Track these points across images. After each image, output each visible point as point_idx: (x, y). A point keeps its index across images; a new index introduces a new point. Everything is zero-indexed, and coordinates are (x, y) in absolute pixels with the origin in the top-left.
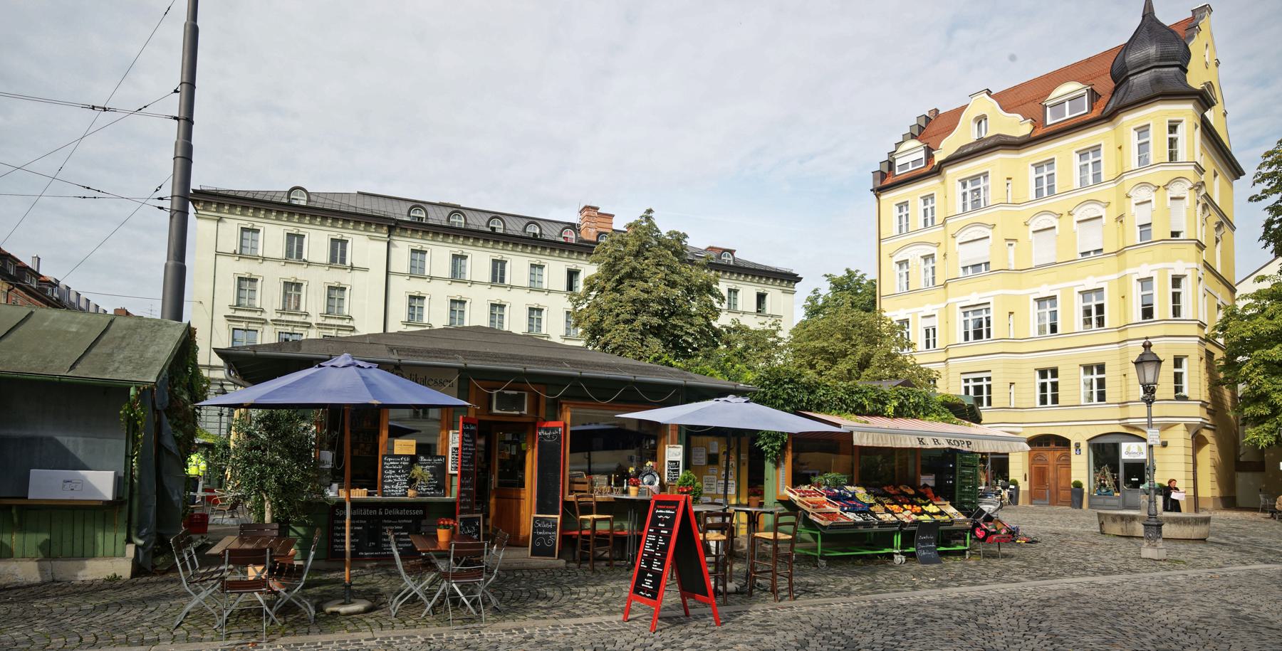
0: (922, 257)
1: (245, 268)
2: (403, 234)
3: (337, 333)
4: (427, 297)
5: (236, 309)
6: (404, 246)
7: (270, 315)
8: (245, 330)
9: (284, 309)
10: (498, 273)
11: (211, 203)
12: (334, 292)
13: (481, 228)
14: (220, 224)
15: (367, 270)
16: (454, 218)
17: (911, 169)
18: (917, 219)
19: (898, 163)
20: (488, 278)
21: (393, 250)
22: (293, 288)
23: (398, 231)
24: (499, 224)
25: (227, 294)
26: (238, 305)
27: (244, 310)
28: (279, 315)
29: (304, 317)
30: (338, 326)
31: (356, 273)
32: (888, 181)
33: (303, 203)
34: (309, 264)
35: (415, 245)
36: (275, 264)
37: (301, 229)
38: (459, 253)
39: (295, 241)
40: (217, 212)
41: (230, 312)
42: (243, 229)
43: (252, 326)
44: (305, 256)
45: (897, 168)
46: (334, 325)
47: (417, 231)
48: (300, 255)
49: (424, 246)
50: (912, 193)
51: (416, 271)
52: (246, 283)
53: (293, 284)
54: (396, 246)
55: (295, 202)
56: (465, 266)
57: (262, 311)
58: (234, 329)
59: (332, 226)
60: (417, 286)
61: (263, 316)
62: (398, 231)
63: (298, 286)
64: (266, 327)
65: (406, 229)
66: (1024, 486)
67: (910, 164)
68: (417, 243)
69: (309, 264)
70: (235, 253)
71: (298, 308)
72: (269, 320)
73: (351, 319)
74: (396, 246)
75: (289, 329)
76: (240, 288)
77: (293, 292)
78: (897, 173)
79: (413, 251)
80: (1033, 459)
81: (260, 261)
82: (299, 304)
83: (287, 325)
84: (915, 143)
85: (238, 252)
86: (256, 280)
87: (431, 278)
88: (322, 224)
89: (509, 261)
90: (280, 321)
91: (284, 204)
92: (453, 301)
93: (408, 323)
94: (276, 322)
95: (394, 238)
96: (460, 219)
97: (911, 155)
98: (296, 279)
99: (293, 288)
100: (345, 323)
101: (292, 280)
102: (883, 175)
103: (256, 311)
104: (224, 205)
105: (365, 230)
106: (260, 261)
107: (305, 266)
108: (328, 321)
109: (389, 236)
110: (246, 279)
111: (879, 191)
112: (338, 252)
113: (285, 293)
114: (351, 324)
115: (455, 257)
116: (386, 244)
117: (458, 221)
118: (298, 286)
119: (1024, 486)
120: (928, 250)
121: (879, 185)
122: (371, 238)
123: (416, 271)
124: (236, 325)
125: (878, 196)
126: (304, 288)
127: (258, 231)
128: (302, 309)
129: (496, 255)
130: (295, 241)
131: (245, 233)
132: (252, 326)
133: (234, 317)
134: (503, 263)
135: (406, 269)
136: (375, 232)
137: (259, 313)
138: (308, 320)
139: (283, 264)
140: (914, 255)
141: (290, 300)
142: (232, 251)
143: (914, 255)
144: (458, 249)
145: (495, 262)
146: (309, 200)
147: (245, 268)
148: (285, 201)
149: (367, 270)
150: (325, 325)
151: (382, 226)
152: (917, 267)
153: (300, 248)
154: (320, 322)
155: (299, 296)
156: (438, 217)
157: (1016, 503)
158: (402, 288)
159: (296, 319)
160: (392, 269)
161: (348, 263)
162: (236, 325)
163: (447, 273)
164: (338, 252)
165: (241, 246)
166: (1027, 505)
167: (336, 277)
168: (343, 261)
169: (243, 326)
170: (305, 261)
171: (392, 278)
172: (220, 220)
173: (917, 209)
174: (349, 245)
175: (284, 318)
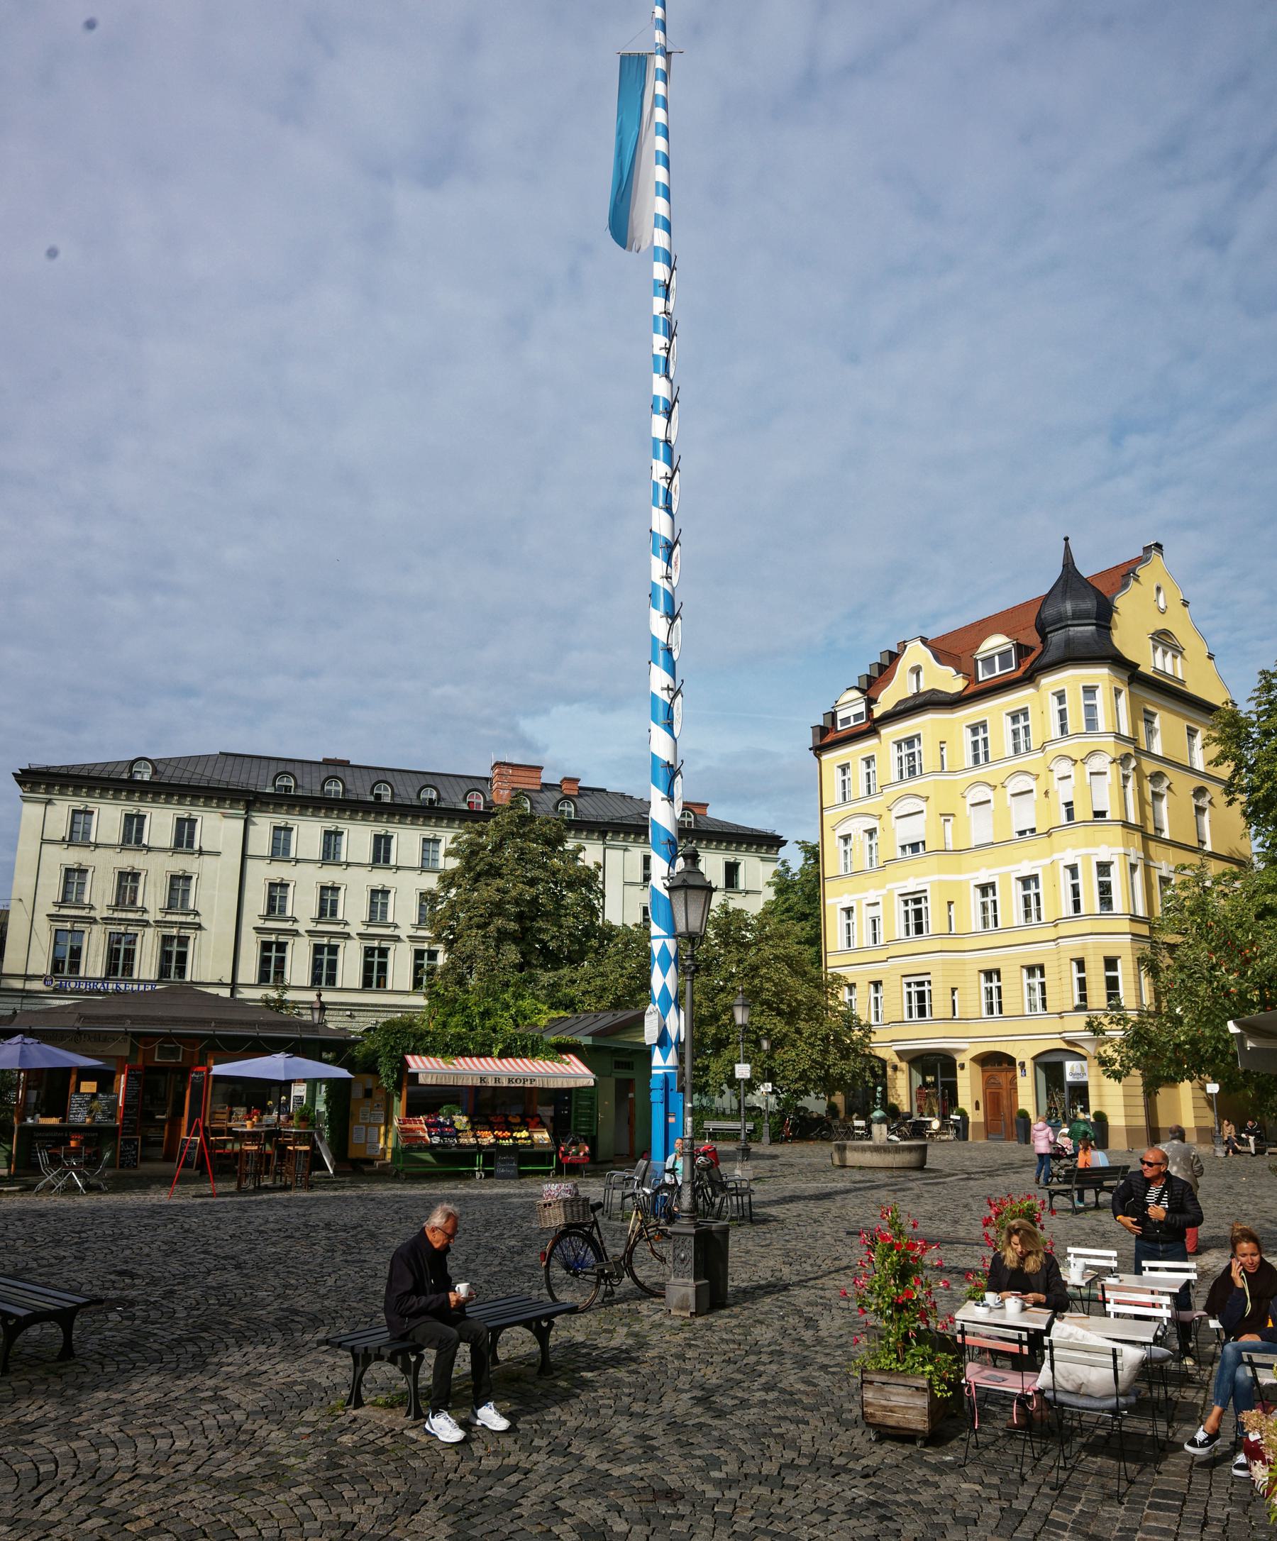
0: (866, 831)
1: (74, 857)
2: (264, 809)
3: (178, 932)
4: (292, 885)
5: (60, 907)
6: (264, 825)
7: (101, 912)
8: (70, 931)
9: (117, 905)
10: (381, 851)
11: (40, 784)
12: (179, 884)
13: (361, 798)
14: (48, 807)
15: (218, 854)
16: (330, 784)
17: (853, 724)
18: (858, 785)
19: (840, 716)
20: (367, 857)
21: (251, 828)
22: (128, 879)
23: (258, 805)
24: (386, 789)
25: (52, 888)
26: (64, 901)
27: (69, 907)
28: (111, 912)
29: (140, 913)
30: (181, 923)
31: (206, 858)
32: (828, 739)
33: (146, 778)
34: (149, 849)
35: (279, 821)
36: (110, 852)
37: (142, 809)
38: (333, 829)
39: (133, 825)
40: (47, 793)
41: (54, 910)
42: (75, 812)
43: (78, 926)
44: (145, 841)
45: (839, 723)
46: (176, 923)
47: (282, 805)
48: (139, 840)
49: (289, 822)
50: (853, 753)
51: (280, 849)
52: (74, 876)
53: (129, 874)
54: (254, 824)
55: (138, 777)
56: (340, 844)
57: (92, 908)
58: (57, 930)
59: (179, 803)
60: (280, 871)
61: (93, 914)
62: (258, 805)
63: (135, 876)
64: (95, 927)
65: (268, 804)
66: (976, 1117)
67: (852, 718)
68: (280, 819)
69: (149, 849)
70: (64, 840)
71: (133, 902)
72: (98, 918)
73: (197, 914)
74: (254, 824)
75: (122, 929)
76: (67, 882)
77: (129, 884)
78: (839, 728)
79: (275, 828)
80: (988, 1083)
81: (92, 848)
82: (135, 898)
83: (120, 924)
84: (856, 694)
85: (67, 839)
86: (86, 871)
87: (298, 861)
88: (167, 802)
89: (395, 836)
90: (111, 919)
91: (123, 780)
92: (323, 888)
93: (266, 918)
94: (106, 920)
95: (254, 814)
96: (337, 785)
97: (851, 707)
98: (134, 868)
99: (128, 879)
100: (189, 919)
101: (129, 870)
102: (822, 731)
103: (84, 908)
104: (54, 785)
105: (218, 807)
106: (92, 848)
107: (145, 852)
108: (169, 918)
109: (247, 813)
110: (74, 870)
111: (819, 750)
112: (184, 836)
113: (120, 886)
114: (197, 920)
115: (328, 834)
116: (242, 822)
117: (335, 789)
118: (135, 876)
119: (976, 1117)
120: (871, 823)
121: (819, 743)
122: (225, 816)
123: (280, 849)
124: (59, 925)
125: (818, 756)
126: (142, 878)
127: (92, 813)
128: (139, 904)
129: (379, 829)
130: (133, 825)
131: (76, 815)
132: (78, 926)
133: (58, 916)
134: (388, 839)
135: (266, 850)
136: (231, 808)
137: (87, 910)
138: (146, 917)
139: (118, 850)
140: (856, 828)
141: (125, 893)
142: (60, 838)
143: (856, 828)
144: (330, 825)
145: (378, 838)
146: (155, 772)
147: (74, 857)
148: (125, 776)
149: (218, 854)
150: (166, 922)
151: (238, 801)
152: (859, 840)
153: (140, 831)
154: (159, 918)
155: (136, 888)
156: (310, 785)
157: (966, 1138)
158: (261, 874)
159: (131, 916)
160: (250, 852)
161: (196, 847)
162: (59, 925)
163: (317, 853)
164: (184, 836)
165: (72, 831)
166: (982, 1141)
167: (180, 863)
168: (190, 844)
169: (68, 926)
170: (144, 846)
171: (250, 862)
172: (49, 802)
173: (858, 771)
174: (198, 825)
175: (117, 915)
